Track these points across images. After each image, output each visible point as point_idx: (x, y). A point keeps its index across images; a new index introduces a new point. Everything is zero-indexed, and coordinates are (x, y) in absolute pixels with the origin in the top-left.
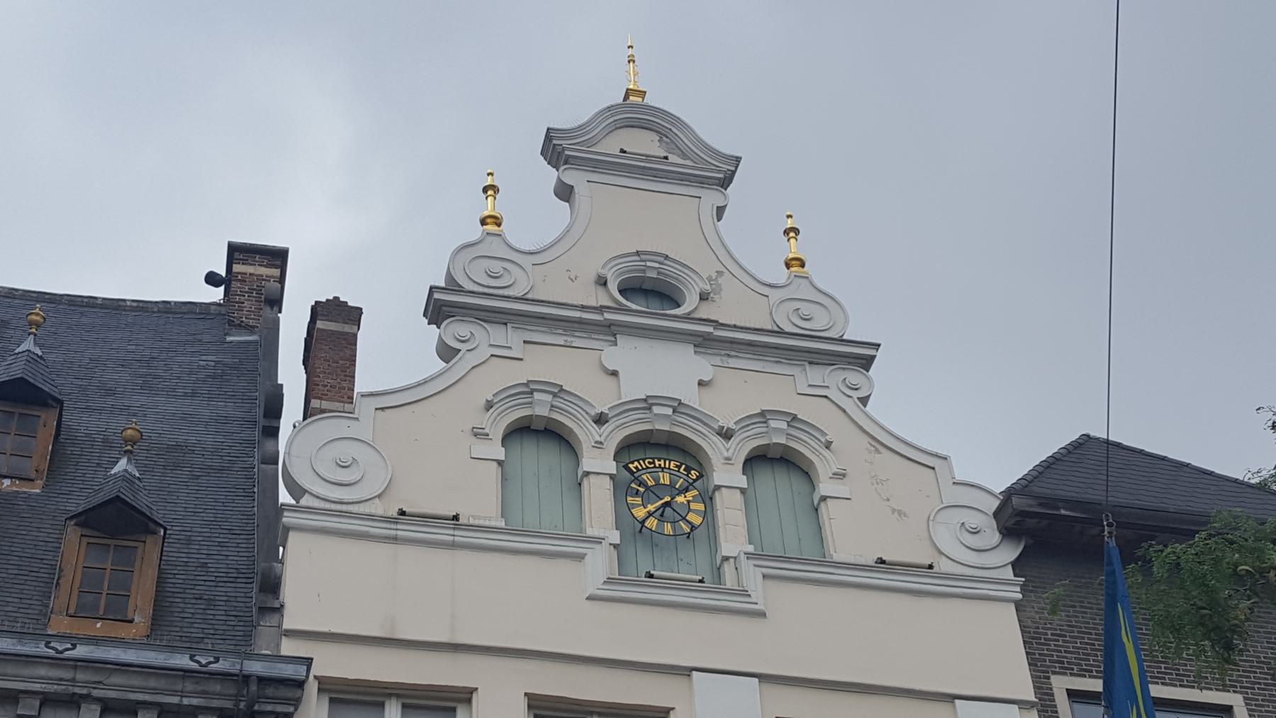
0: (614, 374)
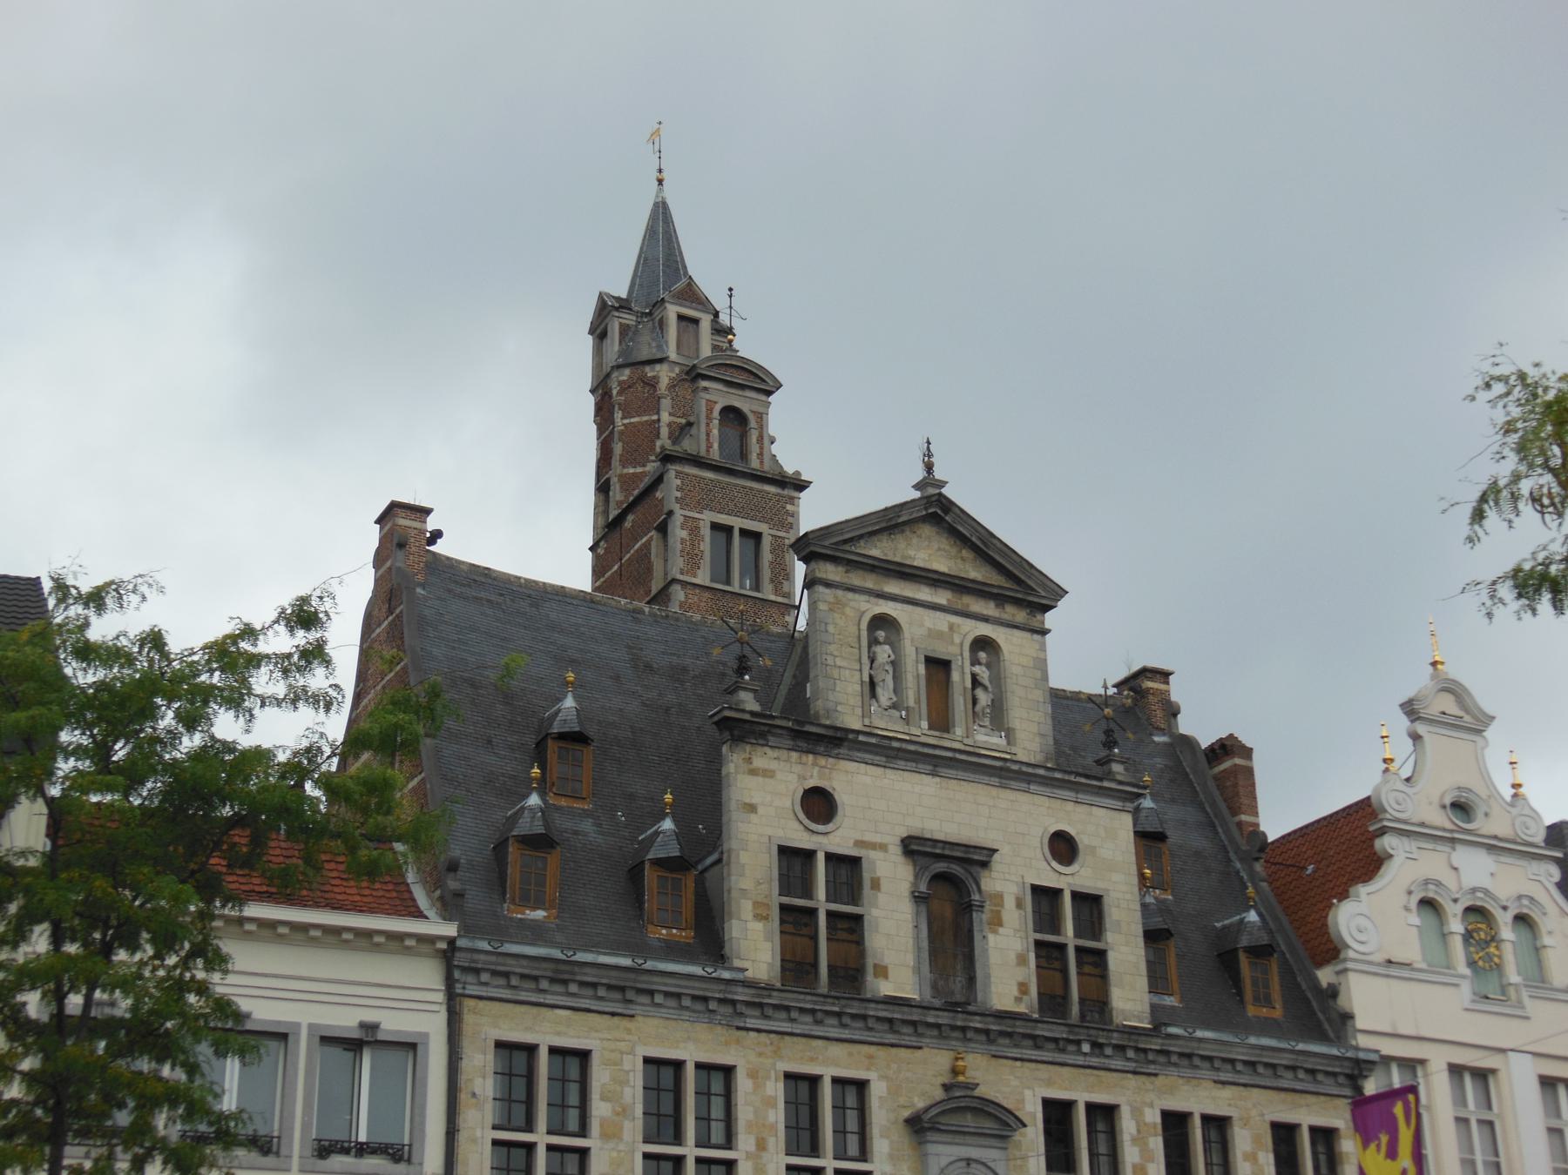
0: (1456, 869)
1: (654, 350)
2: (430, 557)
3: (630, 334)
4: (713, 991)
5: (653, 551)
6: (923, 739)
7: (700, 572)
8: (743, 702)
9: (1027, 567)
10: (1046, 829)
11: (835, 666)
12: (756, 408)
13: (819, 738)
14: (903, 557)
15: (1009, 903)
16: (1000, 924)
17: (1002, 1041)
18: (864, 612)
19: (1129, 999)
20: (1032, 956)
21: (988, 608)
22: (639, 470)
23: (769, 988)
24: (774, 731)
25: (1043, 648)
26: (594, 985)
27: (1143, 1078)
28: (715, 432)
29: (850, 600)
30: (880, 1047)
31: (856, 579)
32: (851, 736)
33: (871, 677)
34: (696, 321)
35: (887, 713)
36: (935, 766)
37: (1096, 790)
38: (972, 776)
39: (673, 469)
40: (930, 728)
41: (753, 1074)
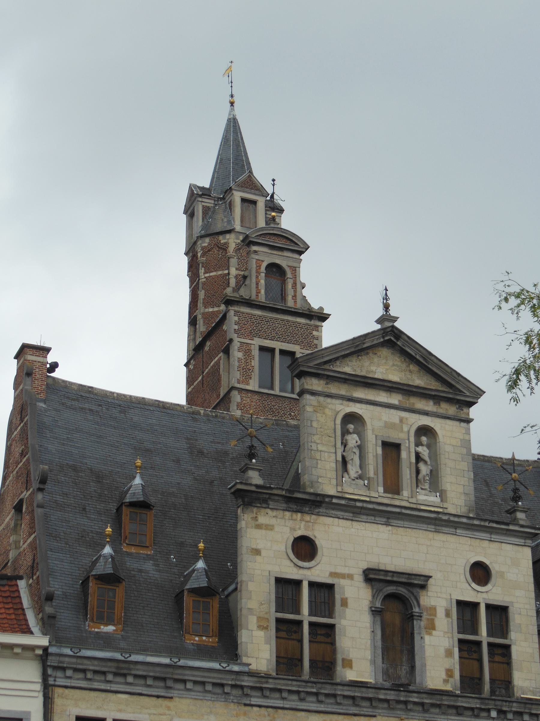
1: (225, 224)
2: (50, 381)
3: (210, 213)
4: (227, 679)
5: (222, 367)
6: (380, 500)
7: (251, 381)
8: (251, 478)
9: (456, 376)
10: (468, 560)
11: (317, 450)
12: (291, 264)
13: (305, 502)
14: (368, 372)
15: (441, 613)
16: (434, 628)
17: (433, 710)
18: (339, 412)
19: (526, 679)
20: (456, 650)
21: (429, 406)
22: (216, 309)
23: (267, 677)
24: (273, 497)
25: (468, 432)
26: (145, 677)
28: (263, 282)
29: (330, 404)
30: (346, 716)
31: (334, 389)
32: (327, 500)
33: (343, 458)
34: (254, 203)
35: (354, 482)
36: (388, 518)
37: (505, 532)
38: (414, 525)
39: (233, 309)
40: (385, 492)
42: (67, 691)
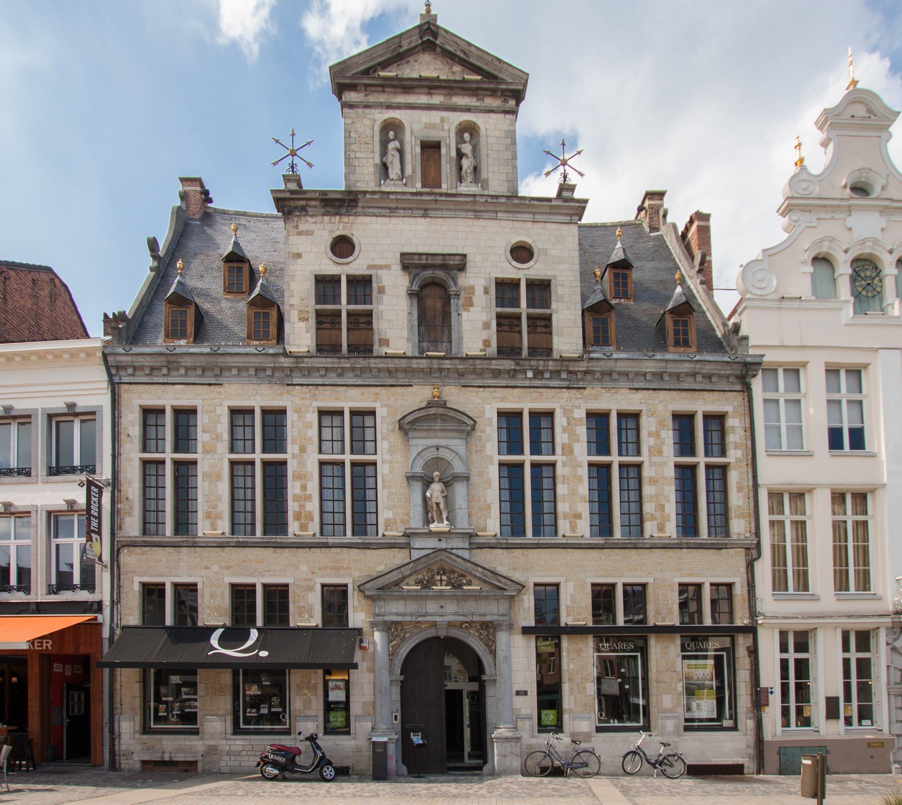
15: (479, 291)
16: (472, 305)
20: (494, 323)
27: (575, 391)
30: (383, 388)
41: (298, 411)
42: (132, 387)
